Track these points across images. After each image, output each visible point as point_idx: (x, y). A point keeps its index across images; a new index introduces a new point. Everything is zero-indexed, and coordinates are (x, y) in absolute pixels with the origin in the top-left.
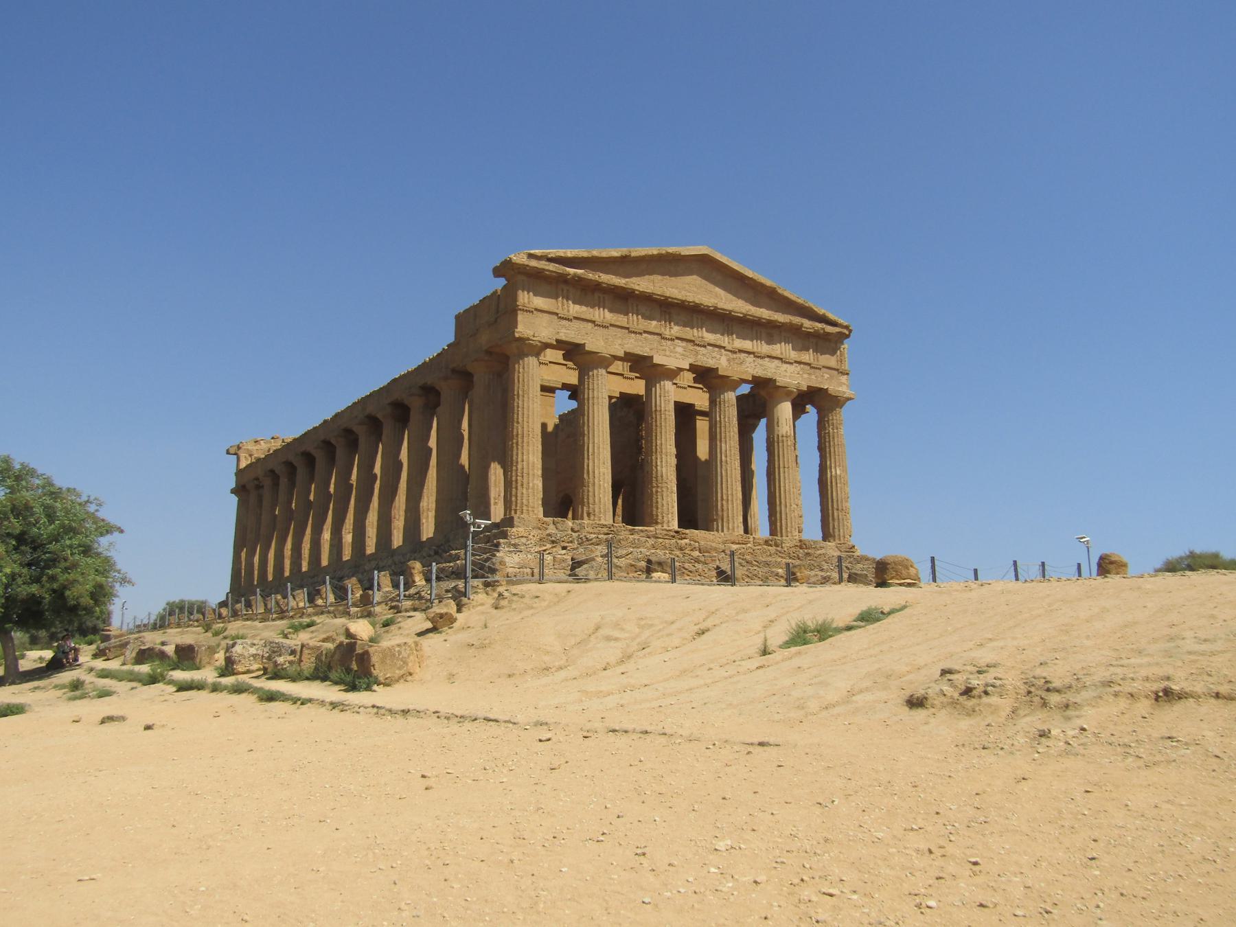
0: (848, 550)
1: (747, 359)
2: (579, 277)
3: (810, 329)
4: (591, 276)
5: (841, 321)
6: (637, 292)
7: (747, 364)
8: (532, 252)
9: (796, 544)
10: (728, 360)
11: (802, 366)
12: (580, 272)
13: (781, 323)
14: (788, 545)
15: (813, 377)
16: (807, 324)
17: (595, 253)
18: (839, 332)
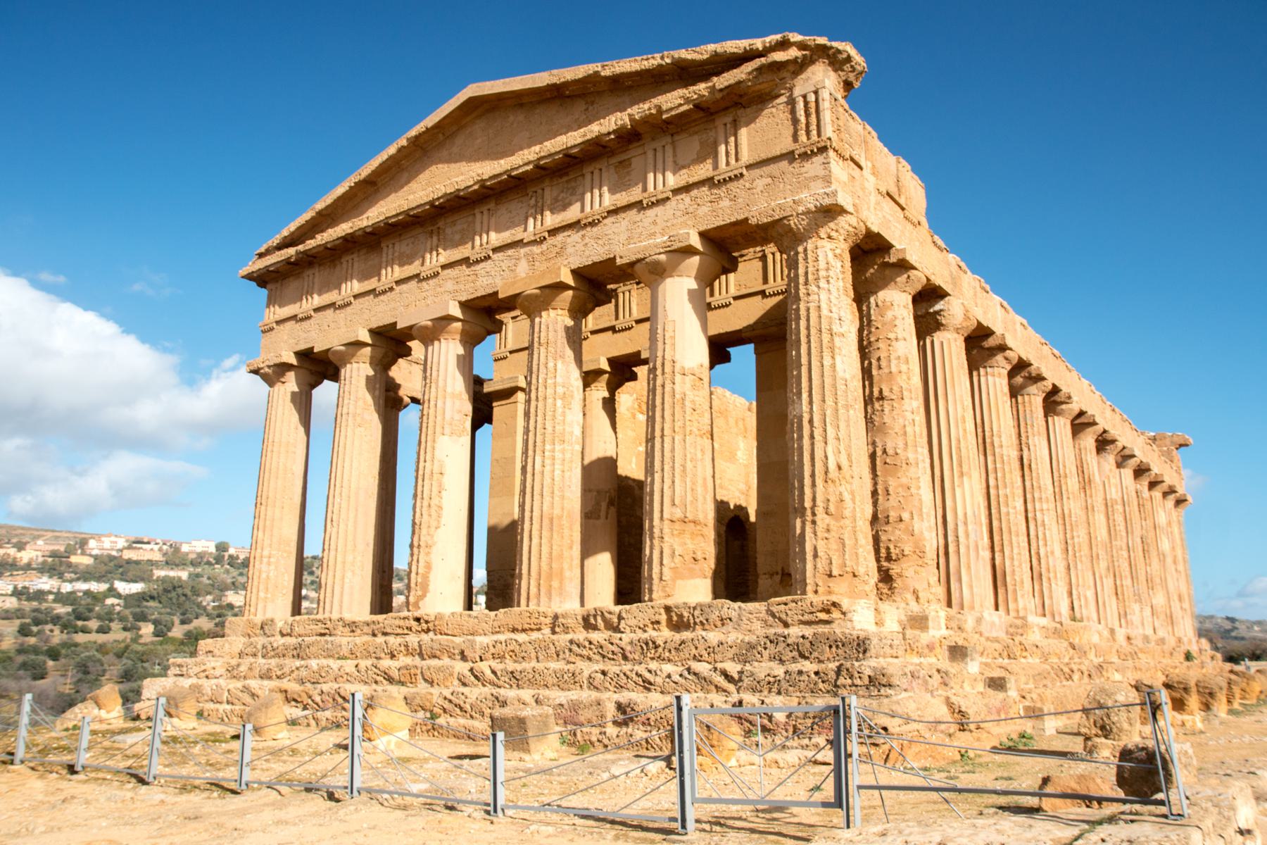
0: (807, 617)
1: (569, 240)
2: (301, 252)
3: (681, 105)
4: (311, 244)
5: (758, 44)
6: (368, 230)
7: (570, 250)
8: (258, 251)
9: (657, 618)
10: (532, 260)
11: (694, 192)
12: (301, 248)
13: (609, 133)
14: (633, 622)
15: (725, 203)
16: (673, 101)
17: (320, 206)
18: (756, 69)
